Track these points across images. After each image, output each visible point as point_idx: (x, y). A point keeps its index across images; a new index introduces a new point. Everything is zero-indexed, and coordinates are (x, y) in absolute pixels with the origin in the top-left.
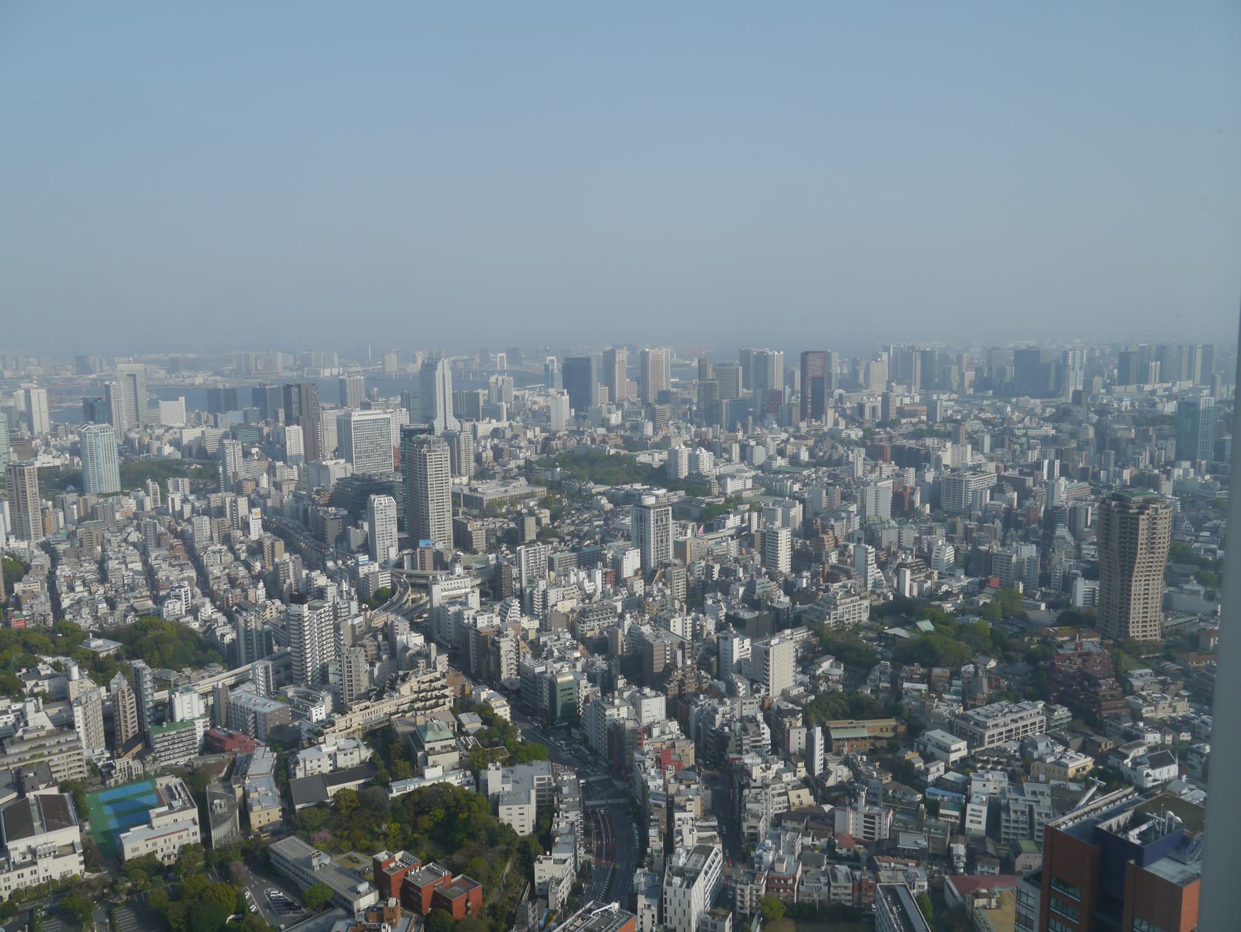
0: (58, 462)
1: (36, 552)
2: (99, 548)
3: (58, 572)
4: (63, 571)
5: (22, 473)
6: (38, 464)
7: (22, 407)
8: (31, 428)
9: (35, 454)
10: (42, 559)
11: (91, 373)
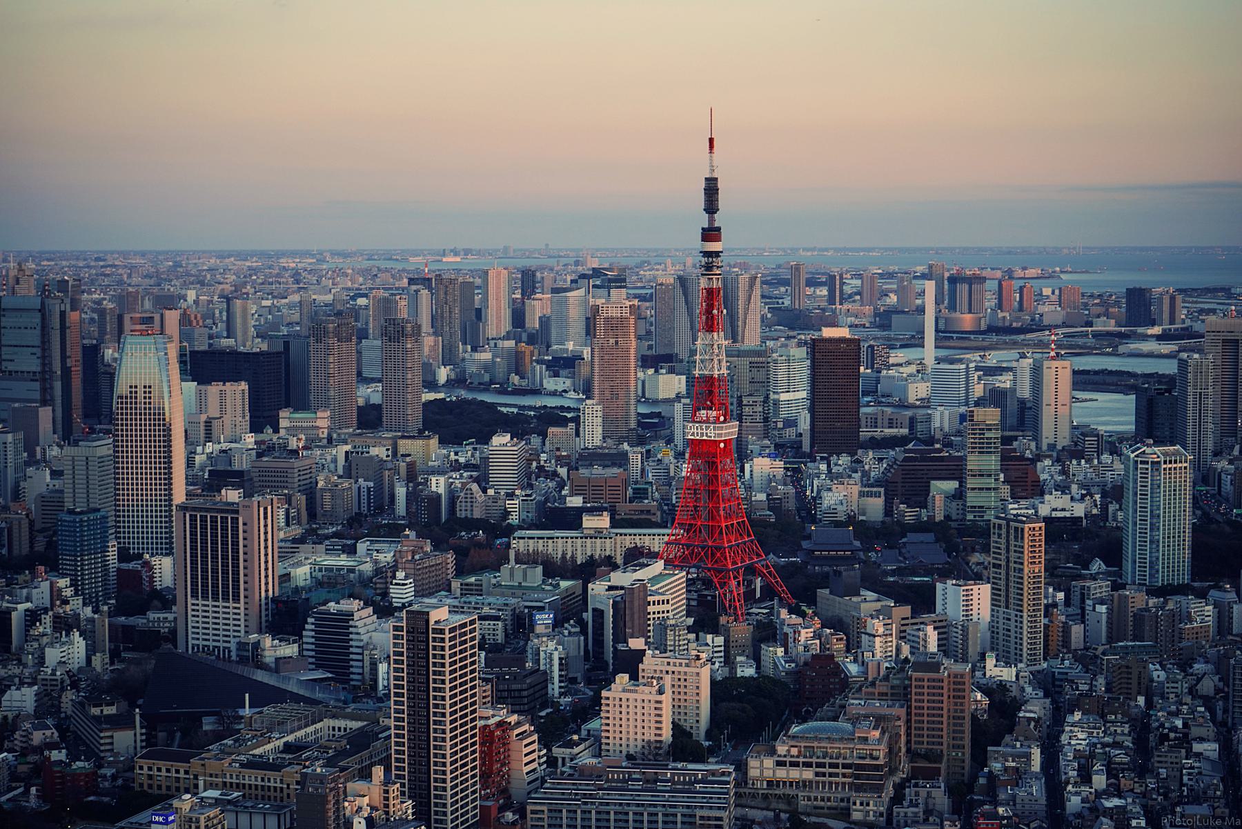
0: (1079, 510)
1: (1029, 689)
2: (1141, 700)
3: (1064, 738)
4: (1077, 736)
5: (1019, 533)
6: (1044, 510)
7: (1025, 392)
8: (1036, 438)
9: (1038, 490)
10: (1035, 708)
11: (1153, 323)
